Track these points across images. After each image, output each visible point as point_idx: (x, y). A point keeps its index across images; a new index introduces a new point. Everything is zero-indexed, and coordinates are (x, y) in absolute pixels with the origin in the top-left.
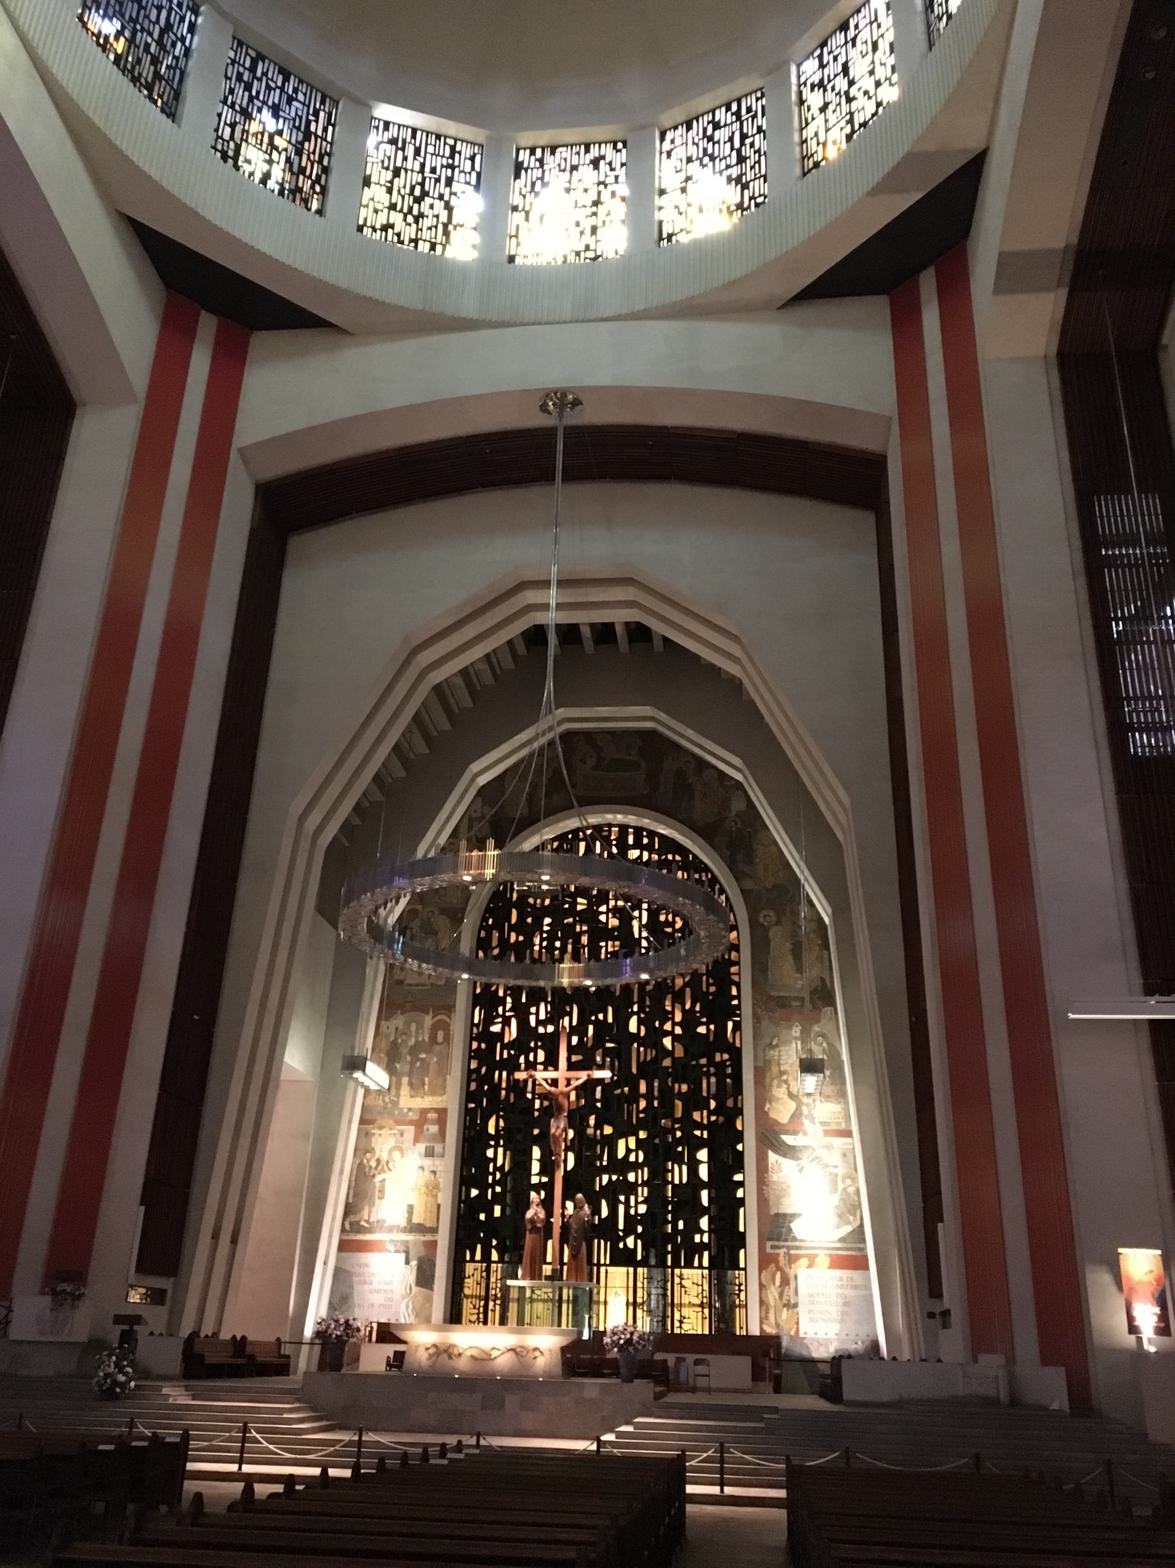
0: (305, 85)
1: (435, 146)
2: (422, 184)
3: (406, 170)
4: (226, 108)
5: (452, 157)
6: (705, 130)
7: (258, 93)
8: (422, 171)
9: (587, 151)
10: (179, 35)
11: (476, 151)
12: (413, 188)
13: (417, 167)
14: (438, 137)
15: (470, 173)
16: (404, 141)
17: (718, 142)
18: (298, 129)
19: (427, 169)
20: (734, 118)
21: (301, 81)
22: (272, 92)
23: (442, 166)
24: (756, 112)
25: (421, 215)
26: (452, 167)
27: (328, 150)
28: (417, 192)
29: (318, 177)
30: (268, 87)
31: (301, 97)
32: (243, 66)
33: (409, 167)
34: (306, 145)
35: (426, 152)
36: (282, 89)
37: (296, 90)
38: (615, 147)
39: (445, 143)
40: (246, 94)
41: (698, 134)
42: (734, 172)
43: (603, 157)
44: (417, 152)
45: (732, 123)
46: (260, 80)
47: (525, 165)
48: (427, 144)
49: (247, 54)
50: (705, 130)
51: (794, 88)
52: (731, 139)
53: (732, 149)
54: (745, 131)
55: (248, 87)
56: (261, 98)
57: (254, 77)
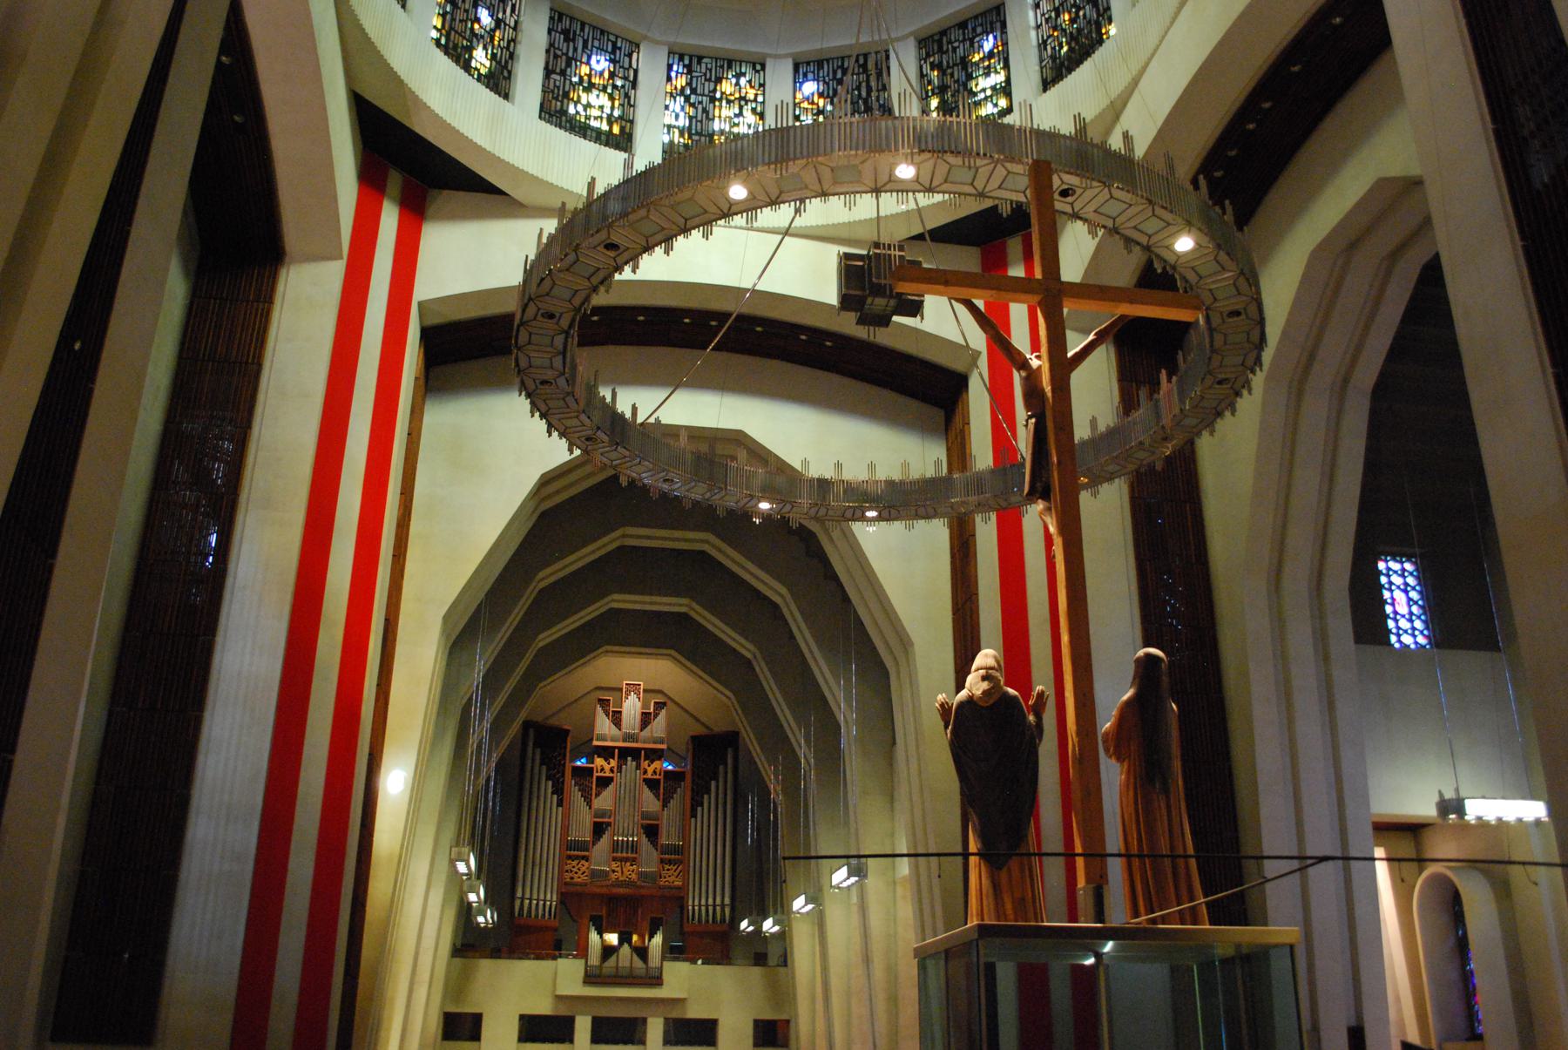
6: (835, 73)
14: (602, 32)
16: (575, 32)
20: (861, 70)
29: (506, 62)
35: (593, 46)
38: (754, 68)
39: (608, 40)
41: (828, 75)
48: (593, 39)
50: (835, 73)
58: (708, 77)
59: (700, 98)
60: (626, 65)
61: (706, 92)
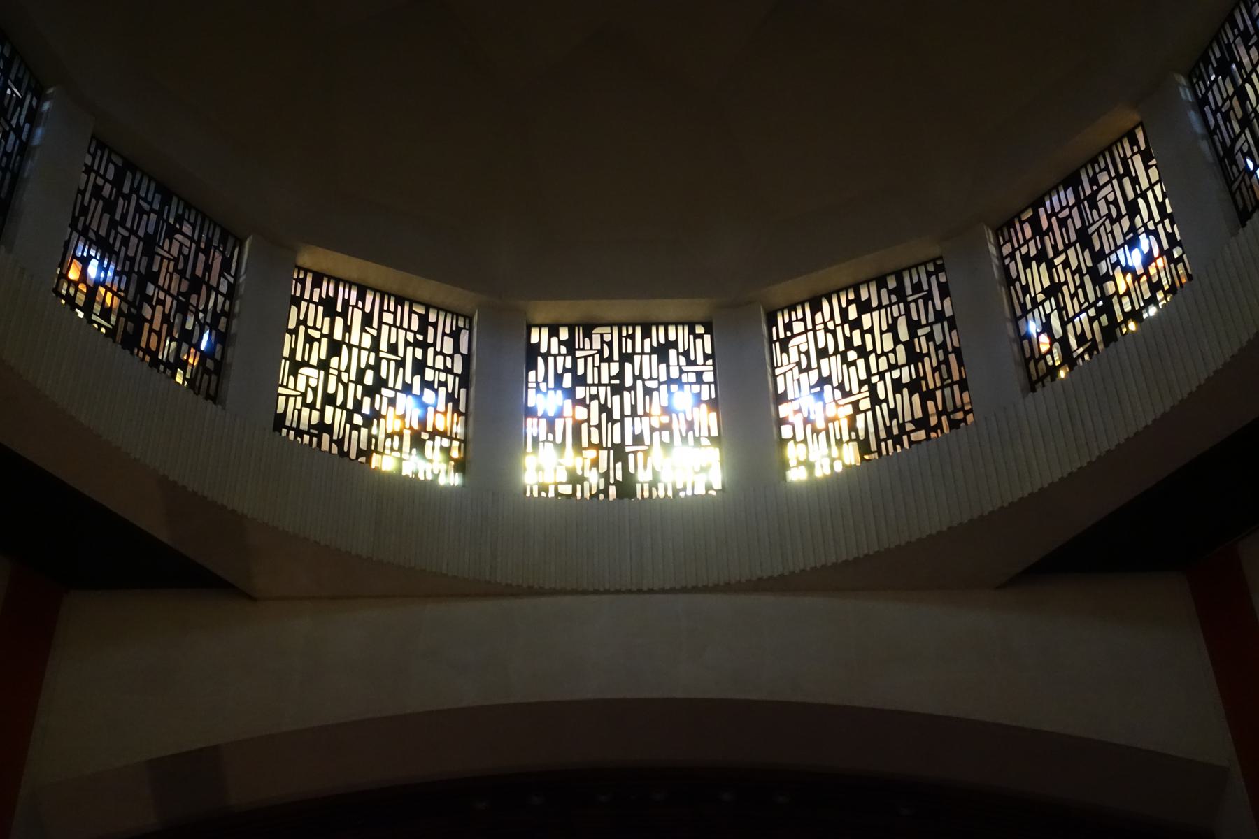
0: (193, 213)
1: (395, 313)
2: (376, 368)
3: (350, 347)
4: (75, 235)
5: (423, 330)
6: (844, 312)
7: (124, 216)
8: (375, 347)
9: (646, 334)
10: (14, 122)
11: (461, 324)
12: (361, 373)
13: (367, 342)
15: (452, 356)
16: (346, 303)
17: (871, 331)
18: (182, 274)
19: (384, 346)
20: (894, 299)
21: (188, 206)
22: (145, 217)
23: (407, 343)
24: (930, 290)
25: (376, 415)
26: (424, 346)
27: (226, 308)
28: (369, 379)
30: (139, 210)
31: (187, 229)
32: (103, 177)
33: (355, 341)
34: (194, 300)
35: (381, 322)
36: (159, 214)
37: (180, 219)
38: (692, 331)
39: (411, 312)
40: (106, 217)
41: (832, 318)
42: (906, 375)
43: (674, 345)
44: (367, 320)
45: (891, 305)
46: (127, 198)
47: (543, 349)
48: (381, 311)
49: (109, 161)
50: (844, 312)
51: (996, 261)
52: (892, 328)
53: (897, 341)
54: (915, 317)
55: (110, 207)
56: (128, 225)
57: (120, 193)
58: (606, 354)
59: (594, 391)
60: (448, 349)
61: (605, 380)
